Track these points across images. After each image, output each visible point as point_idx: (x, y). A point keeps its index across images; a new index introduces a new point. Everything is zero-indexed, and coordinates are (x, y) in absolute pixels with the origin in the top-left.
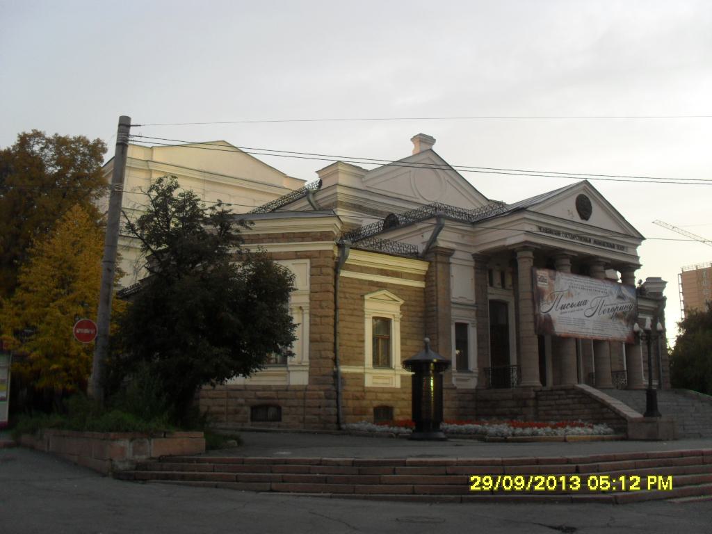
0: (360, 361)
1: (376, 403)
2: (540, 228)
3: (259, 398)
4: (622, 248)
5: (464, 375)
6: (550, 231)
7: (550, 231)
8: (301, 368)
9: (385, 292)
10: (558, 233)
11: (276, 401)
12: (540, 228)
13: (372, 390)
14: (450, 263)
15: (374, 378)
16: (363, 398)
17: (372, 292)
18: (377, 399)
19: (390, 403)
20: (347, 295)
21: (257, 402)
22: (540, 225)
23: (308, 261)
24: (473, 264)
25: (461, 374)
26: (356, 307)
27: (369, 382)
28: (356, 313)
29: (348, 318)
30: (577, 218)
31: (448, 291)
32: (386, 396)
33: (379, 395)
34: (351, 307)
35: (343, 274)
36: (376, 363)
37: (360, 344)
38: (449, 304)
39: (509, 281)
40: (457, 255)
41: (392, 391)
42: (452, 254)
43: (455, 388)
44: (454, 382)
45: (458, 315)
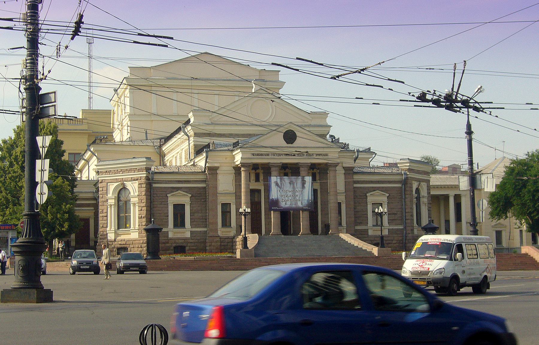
0: (167, 226)
1: (174, 245)
2: (253, 155)
3: (120, 245)
4: (327, 155)
5: (228, 229)
6: (258, 155)
7: (262, 155)
8: (135, 231)
9: (179, 191)
10: (268, 155)
11: (125, 246)
12: (253, 155)
13: (171, 239)
14: (217, 173)
15: (175, 233)
16: (168, 243)
17: (172, 192)
18: (175, 243)
19: (184, 244)
20: (158, 195)
21: (119, 246)
22: (252, 153)
23: (137, 182)
24: (234, 171)
25: (224, 229)
26: (164, 200)
27: (170, 235)
28: (163, 203)
29: (159, 206)
30: (284, 143)
31: (216, 187)
32: (181, 241)
33: (177, 241)
34: (160, 200)
35: (155, 185)
36: (176, 225)
37: (167, 218)
38: (216, 194)
39: (261, 177)
40: (220, 169)
41: (185, 239)
42: (218, 169)
43: (219, 236)
44: (220, 233)
45: (222, 199)
